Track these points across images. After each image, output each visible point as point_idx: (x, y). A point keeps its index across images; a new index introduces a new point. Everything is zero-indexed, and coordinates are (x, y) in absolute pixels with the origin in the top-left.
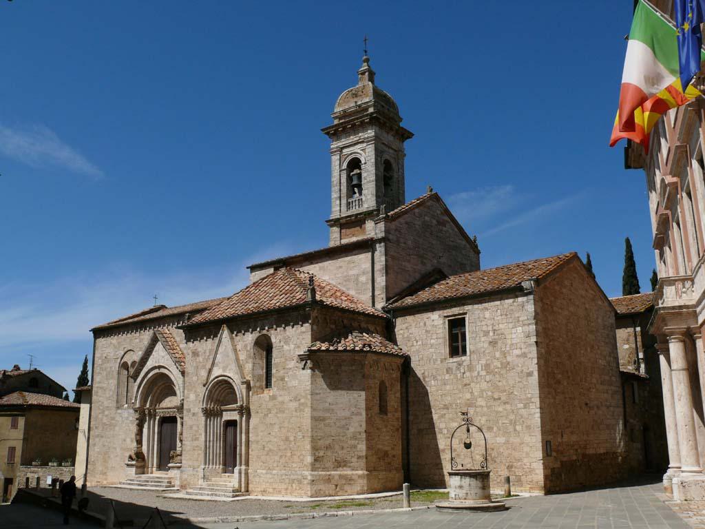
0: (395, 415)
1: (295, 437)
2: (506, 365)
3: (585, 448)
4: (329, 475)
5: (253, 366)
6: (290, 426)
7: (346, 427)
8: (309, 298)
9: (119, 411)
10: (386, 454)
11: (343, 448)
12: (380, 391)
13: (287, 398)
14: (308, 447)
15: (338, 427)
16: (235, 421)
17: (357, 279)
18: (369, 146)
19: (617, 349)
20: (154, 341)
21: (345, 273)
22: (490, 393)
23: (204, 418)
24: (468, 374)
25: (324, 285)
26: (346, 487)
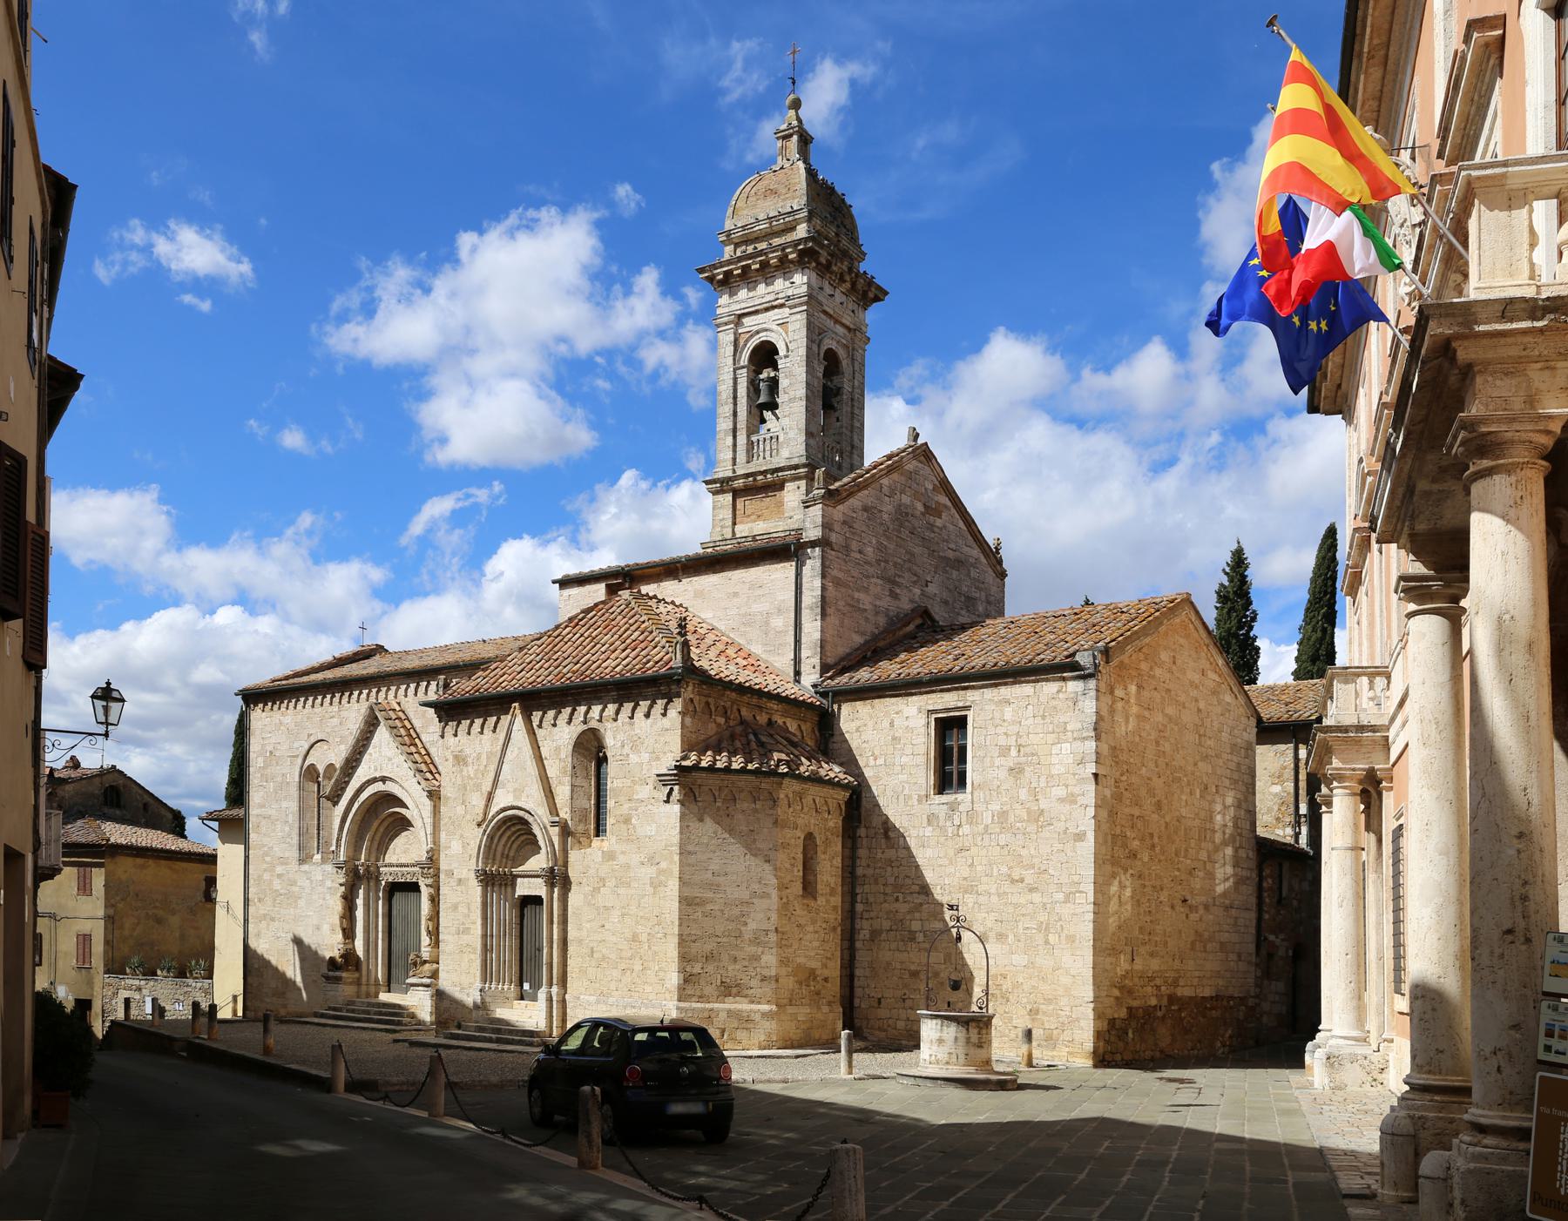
0: (830, 901)
1: (649, 934)
2: (1037, 816)
3: (1175, 983)
4: (712, 1010)
5: (572, 791)
6: (641, 914)
7: (742, 919)
8: (677, 662)
9: (305, 867)
10: (812, 972)
11: (735, 960)
12: (805, 853)
13: (635, 859)
14: (675, 954)
15: (728, 920)
16: (536, 901)
17: (767, 623)
19: (1254, 794)
20: (371, 724)
21: (743, 611)
22: (1004, 869)
23: (479, 890)
24: (966, 829)
25: (702, 631)
26: (740, 1035)
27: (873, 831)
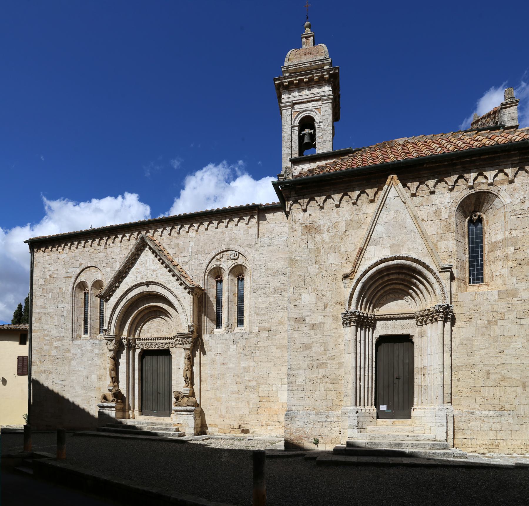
18: (324, 105)
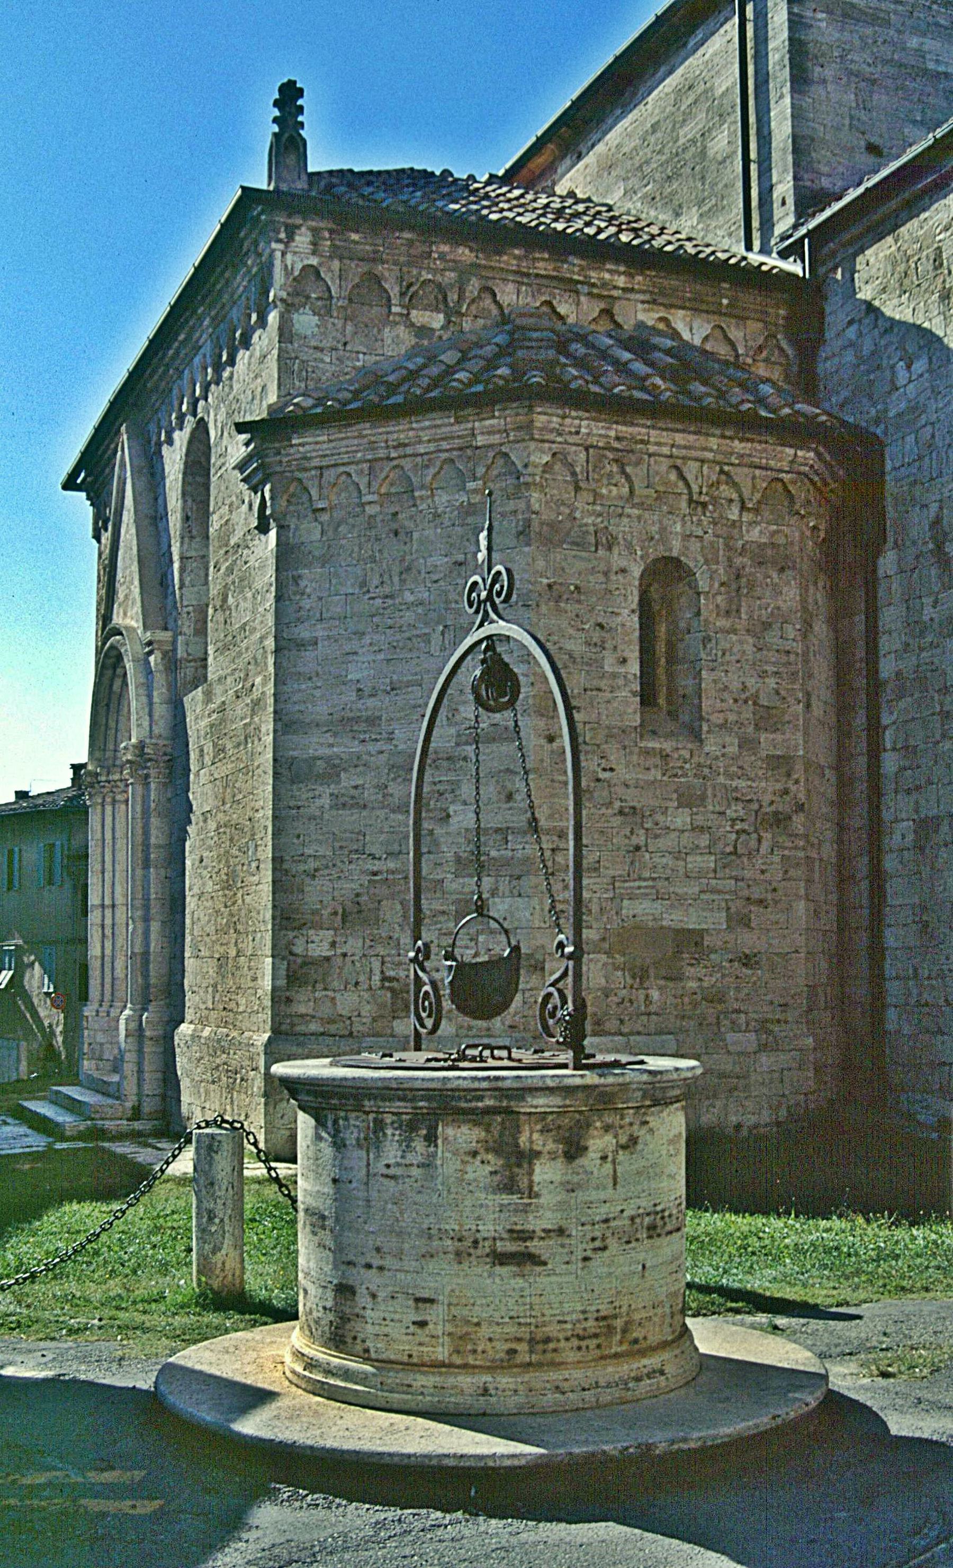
27: (912, 551)
